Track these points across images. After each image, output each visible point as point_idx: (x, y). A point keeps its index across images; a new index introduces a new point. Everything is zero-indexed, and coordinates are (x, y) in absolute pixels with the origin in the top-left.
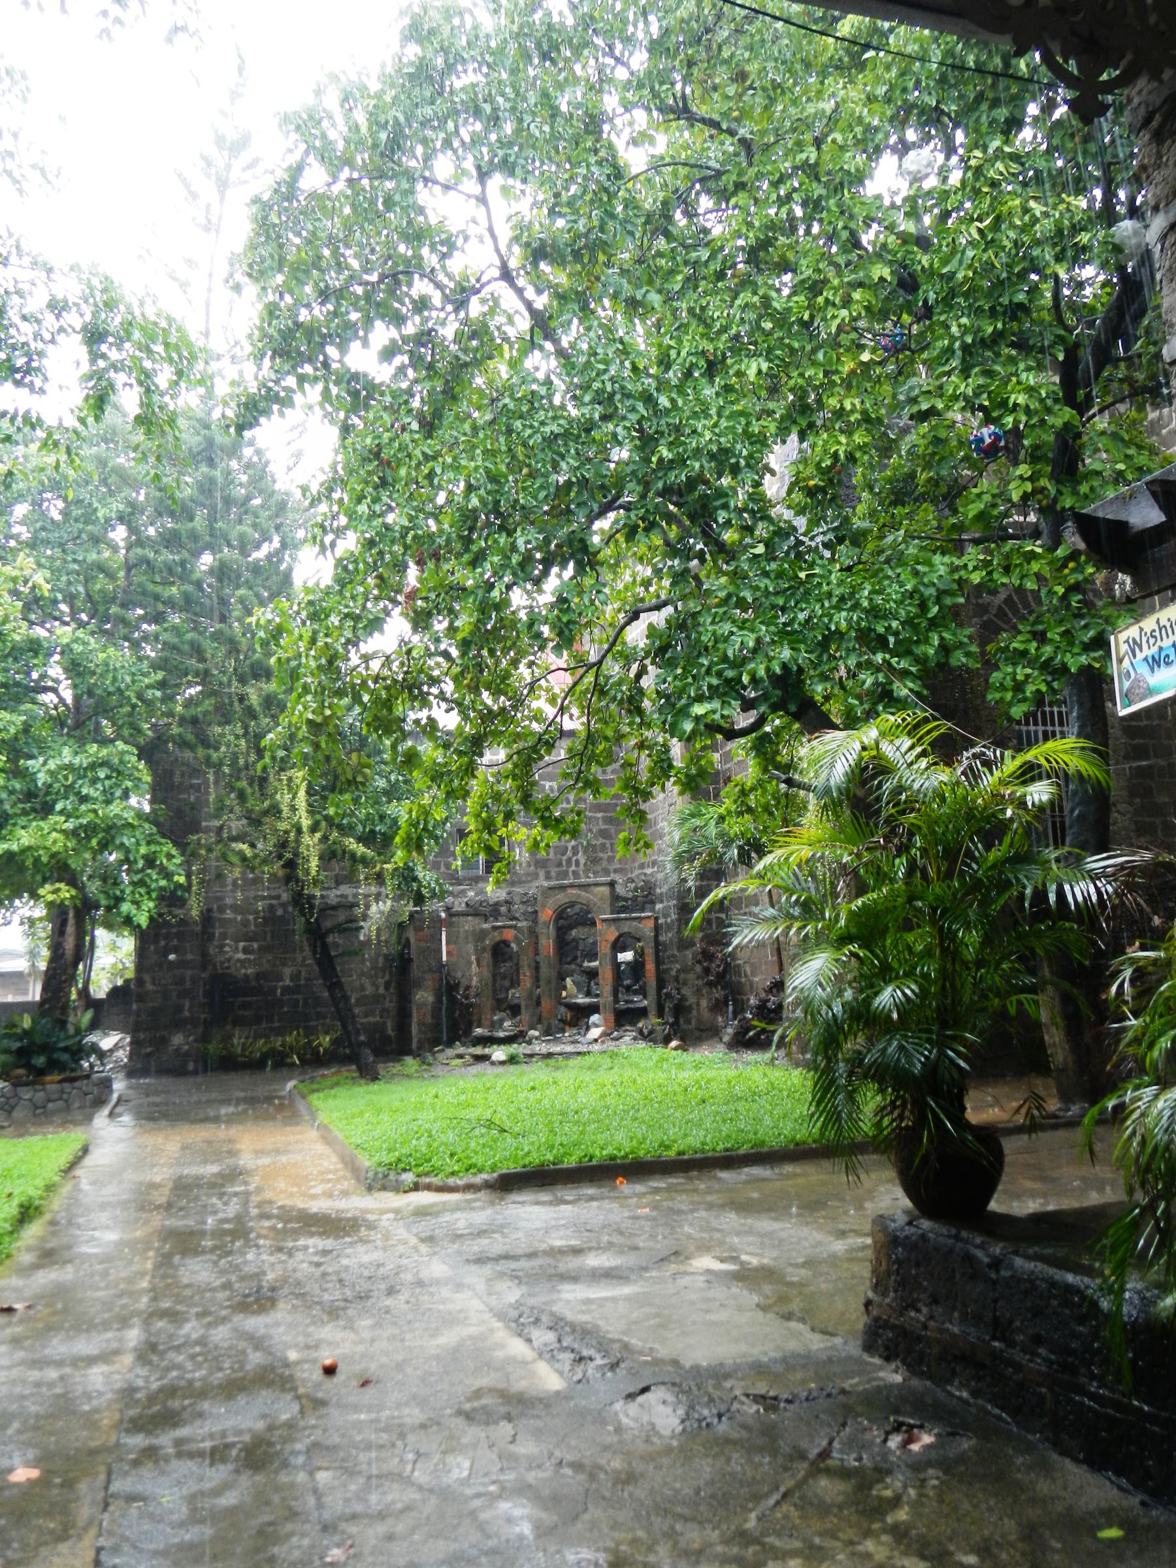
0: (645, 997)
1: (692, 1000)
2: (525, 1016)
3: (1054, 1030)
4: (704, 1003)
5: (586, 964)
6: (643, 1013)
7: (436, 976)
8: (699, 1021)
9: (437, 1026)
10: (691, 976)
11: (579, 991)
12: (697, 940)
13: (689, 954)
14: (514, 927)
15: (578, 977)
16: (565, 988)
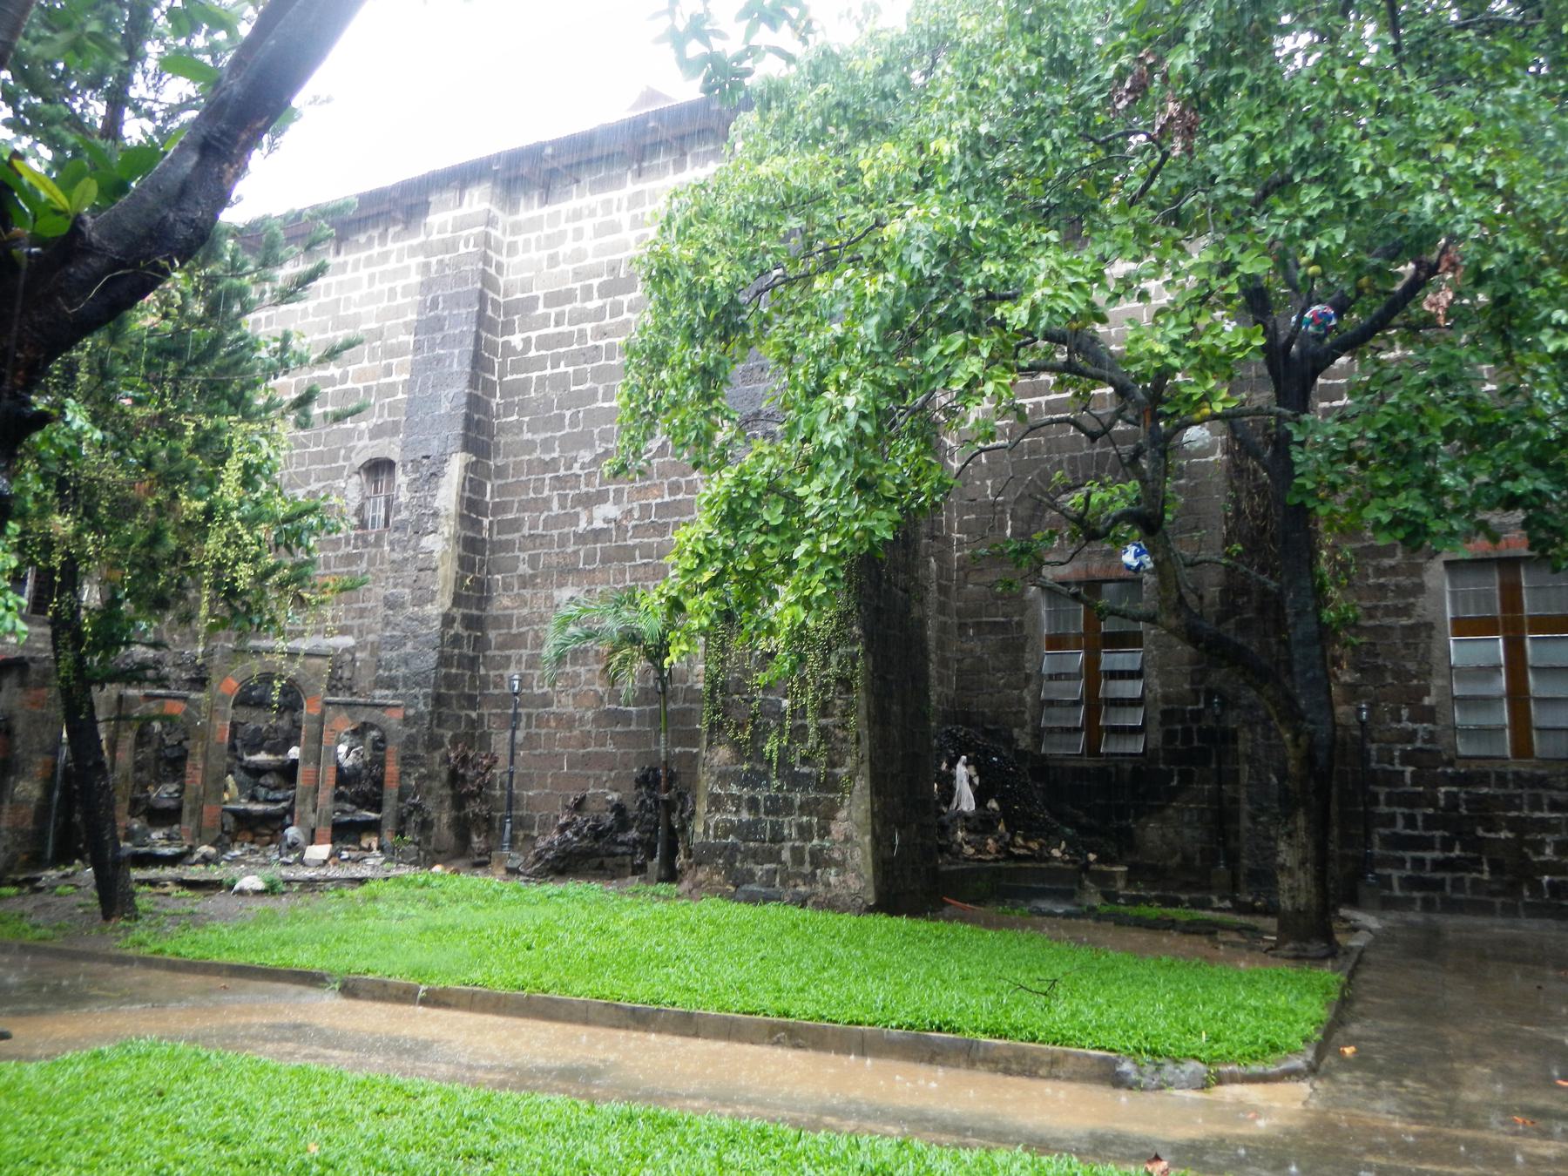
0: (377, 806)
1: (434, 815)
2: (187, 825)
3: (1300, 875)
4: (445, 818)
5: (247, 758)
6: (373, 827)
7: (48, 758)
8: (438, 840)
9: (39, 836)
10: (436, 784)
11: (241, 792)
12: (446, 740)
13: (437, 756)
14: (185, 699)
15: (242, 776)
16: (226, 789)
